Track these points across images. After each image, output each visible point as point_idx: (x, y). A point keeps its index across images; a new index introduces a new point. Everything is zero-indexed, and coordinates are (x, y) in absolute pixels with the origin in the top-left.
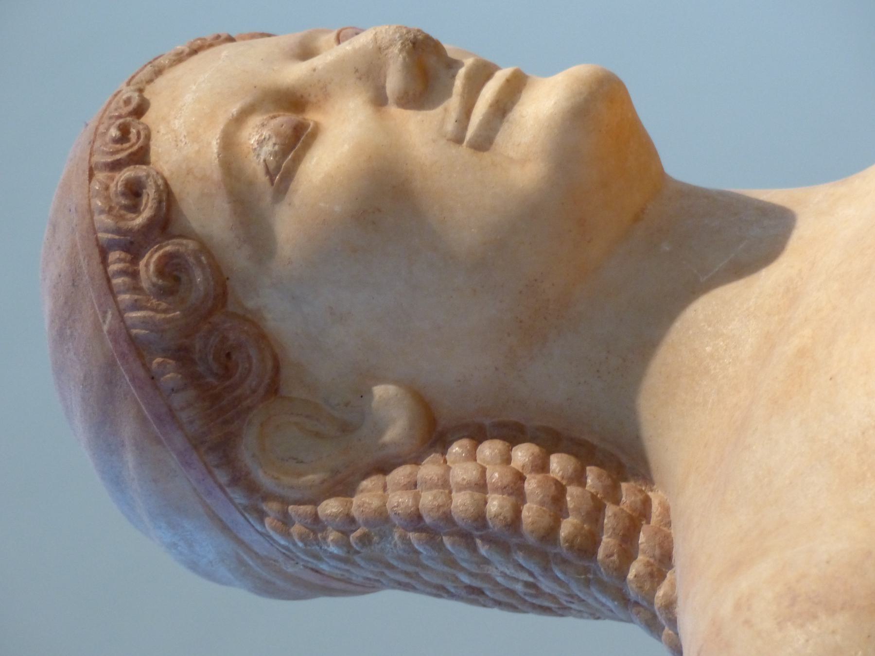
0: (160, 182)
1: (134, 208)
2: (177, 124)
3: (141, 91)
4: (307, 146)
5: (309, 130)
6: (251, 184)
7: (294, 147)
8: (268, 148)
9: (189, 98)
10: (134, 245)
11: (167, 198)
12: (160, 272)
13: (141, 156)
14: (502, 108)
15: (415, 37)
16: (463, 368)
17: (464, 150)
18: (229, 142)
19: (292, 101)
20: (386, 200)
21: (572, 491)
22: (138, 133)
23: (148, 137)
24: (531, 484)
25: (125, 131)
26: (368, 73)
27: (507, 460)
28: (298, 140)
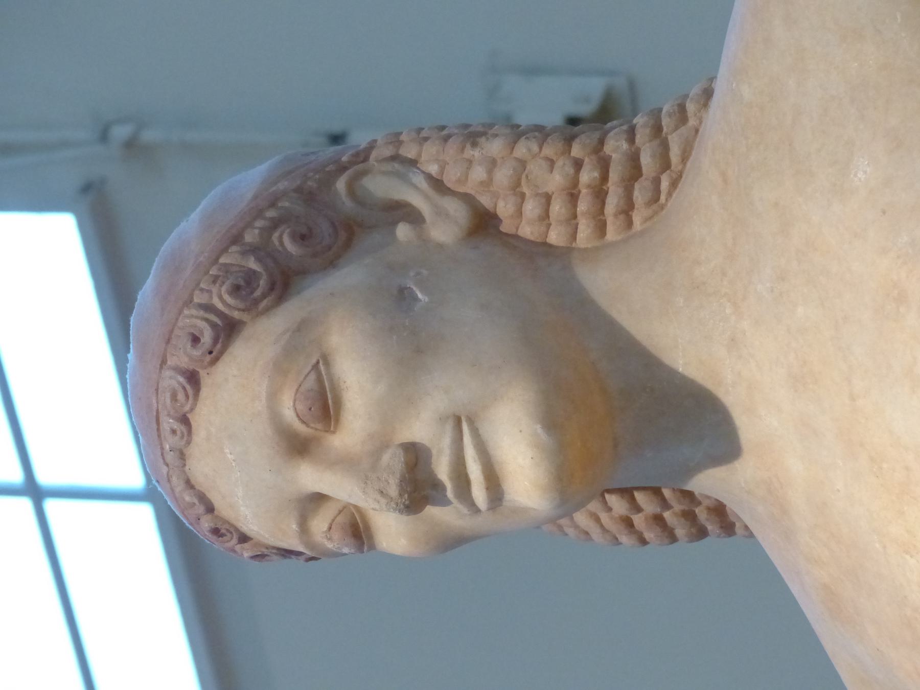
0: (274, 551)
2: (255, 528)
3: (189, 484)
4: (370, 537)
5: (361, 525)
7: (363, 543)
13: (244, 538)
15: (404, 504)
21: (667, 515)
22: (227, 530)
23: (237, 530)
24: (638, 520)
25: (216, 532)
27: (609, 509)
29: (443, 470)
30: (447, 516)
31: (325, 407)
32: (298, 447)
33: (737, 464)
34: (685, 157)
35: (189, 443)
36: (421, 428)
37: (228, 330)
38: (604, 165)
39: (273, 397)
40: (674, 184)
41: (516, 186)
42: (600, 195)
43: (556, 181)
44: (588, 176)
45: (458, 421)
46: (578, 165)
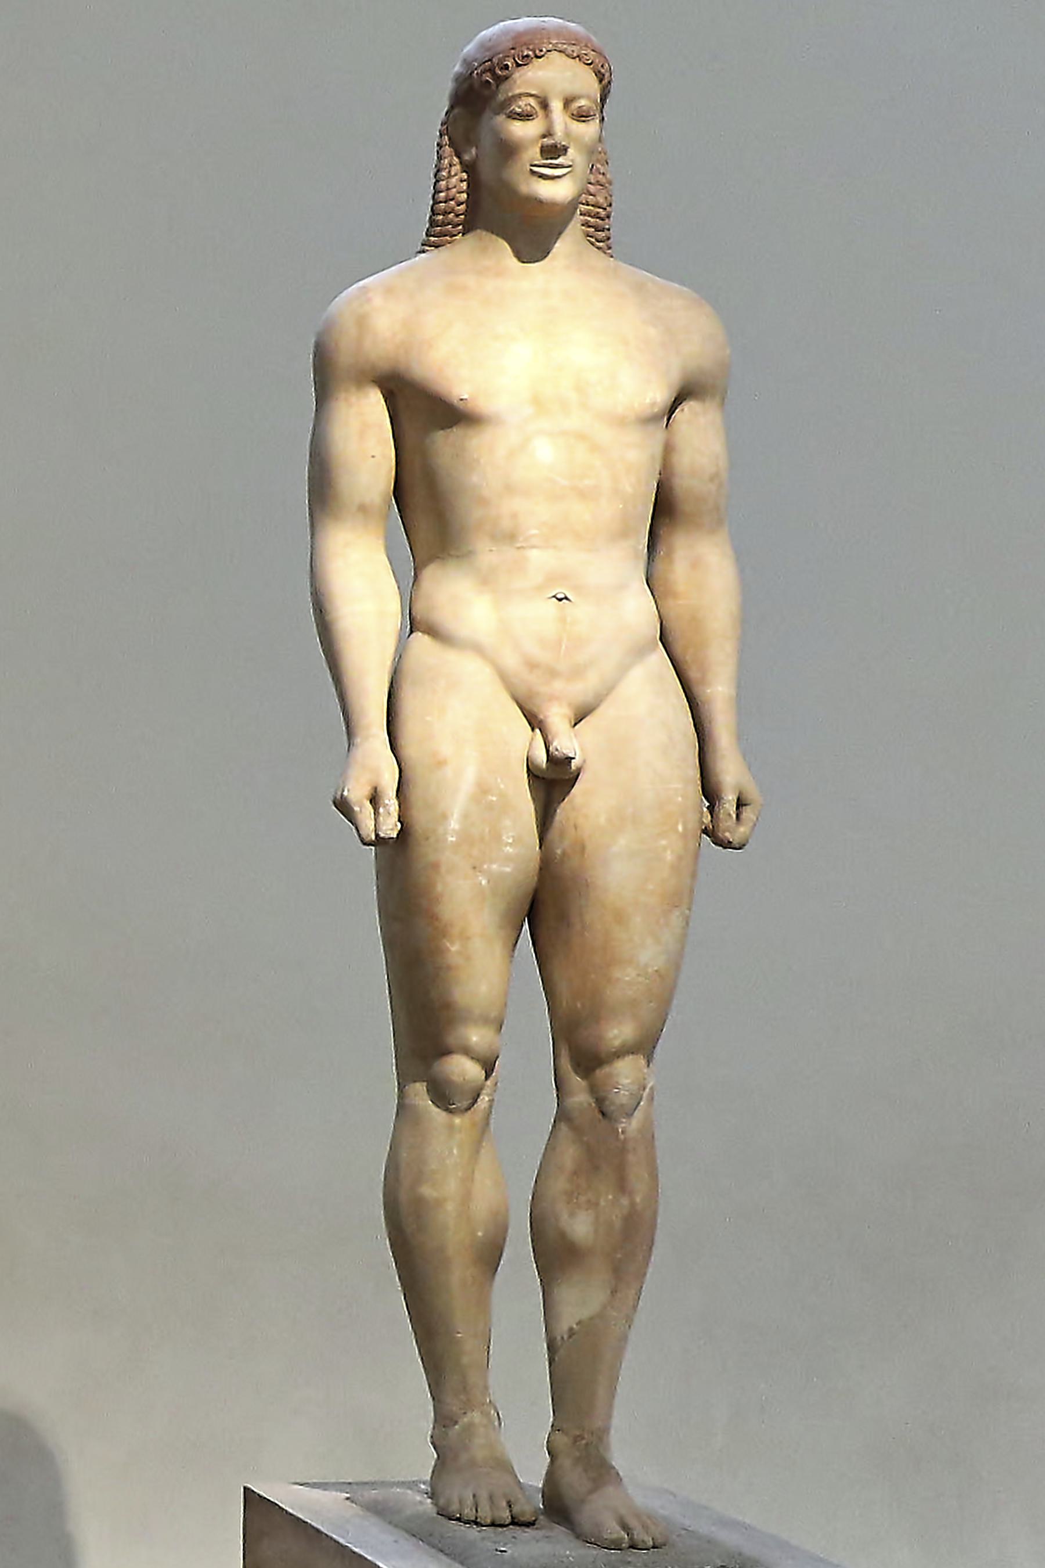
1: (501, 69)
2: (530, 74)
6: (510, 105)
8: (519, 110)
9: (540, 73)
10: (491, 70)
11: (507, 78)
12: (487, 81)
14: (542, 176)
16: (486, 171)
17: (529, 167)
18: (520, 96)
19: (545, 105)
20: (508, 150)
25: (527, 56)
26: (548, 134)
28: (526, 116)
29: (560, 161)
30: (533, 153)
31: (582, 116)
32: (567, 102)
33: (515, 260)
34: (599, 248)
35: (568, 56)
36: (570, 151)
37: (601, 81)
38: (602, 219)
39: (588, 97)
40: (592, 244)
41: (598, 183)
42: (596, 216)
43: (601, 200)
44: (603, 213)
45: (570, 166)
46: (605, 209)
